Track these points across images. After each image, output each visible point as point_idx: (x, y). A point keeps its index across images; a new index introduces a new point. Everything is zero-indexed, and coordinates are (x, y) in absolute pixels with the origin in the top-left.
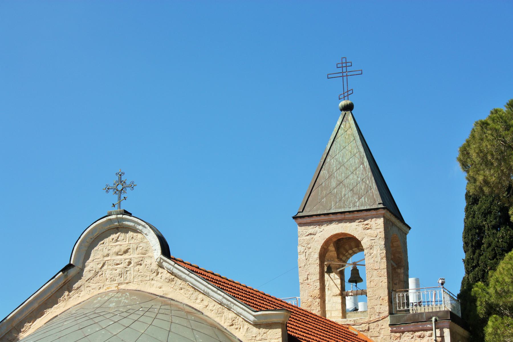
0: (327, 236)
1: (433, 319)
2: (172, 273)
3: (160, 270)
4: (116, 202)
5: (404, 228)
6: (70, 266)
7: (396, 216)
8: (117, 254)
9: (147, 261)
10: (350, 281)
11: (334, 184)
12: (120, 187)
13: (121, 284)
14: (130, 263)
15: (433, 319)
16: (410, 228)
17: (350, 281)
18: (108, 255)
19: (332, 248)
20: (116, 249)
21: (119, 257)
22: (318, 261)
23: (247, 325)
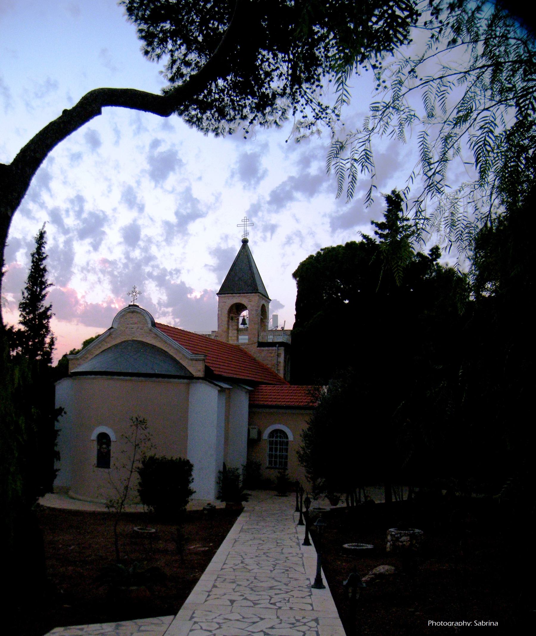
0: (232, 303)
1: (277, 345)
2: (156, 334)
3: (151, 333)
4: (132, 300)
5: (268, 300)
6: (112, 328)
7: (264, 296)
8: (131, 324)
9: (145, 328)
10: (241, 324)
11: (237, 279)
12: (134, 294)
13: (134, 337)
14: (138, 328)
15: (277, 345)
16: (270, 300)
17: (241, 324)
18: (128, 324)
19: (234, 308)
20: (131, 322)
21: (132, 325)
22: (227, 315)
23: (187, 361)
